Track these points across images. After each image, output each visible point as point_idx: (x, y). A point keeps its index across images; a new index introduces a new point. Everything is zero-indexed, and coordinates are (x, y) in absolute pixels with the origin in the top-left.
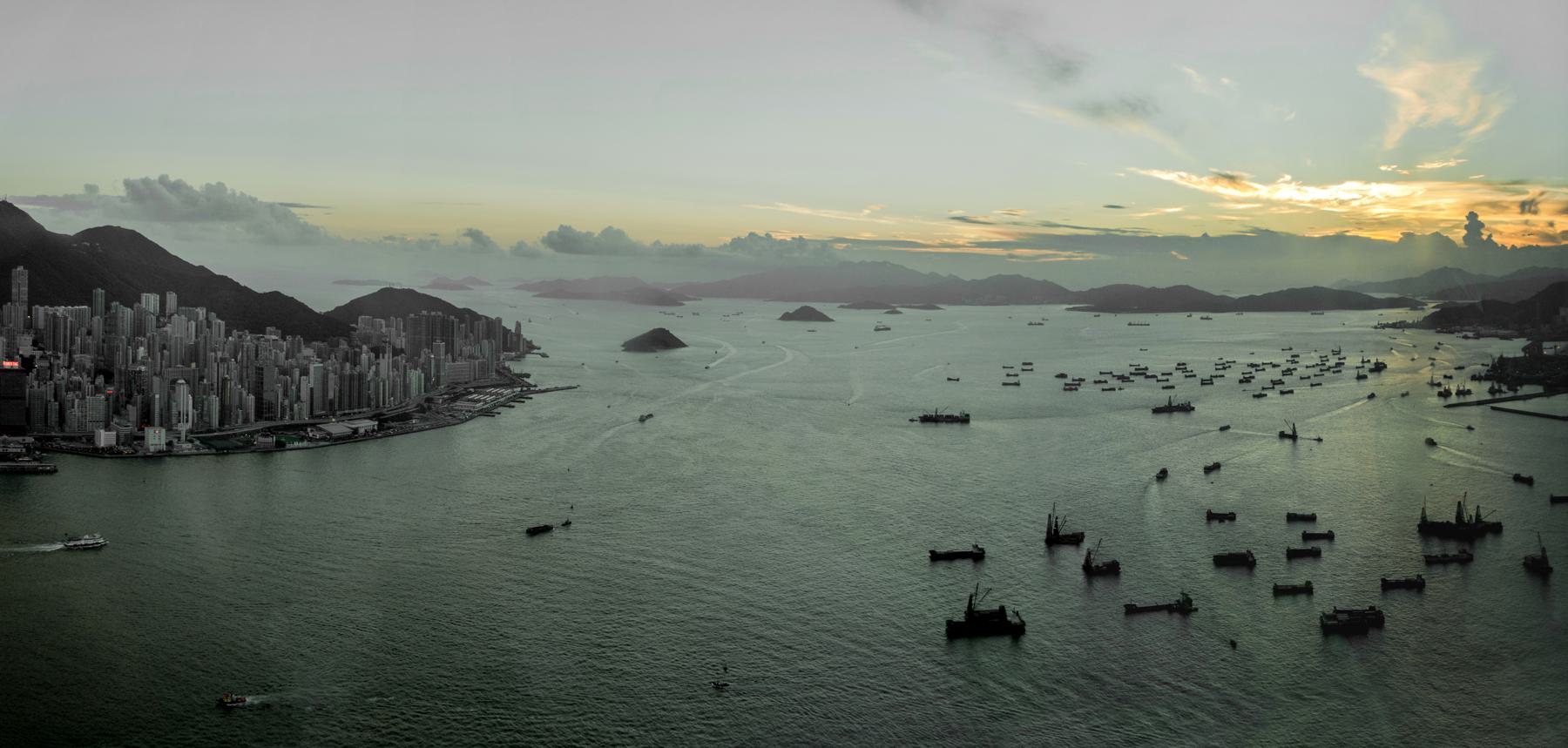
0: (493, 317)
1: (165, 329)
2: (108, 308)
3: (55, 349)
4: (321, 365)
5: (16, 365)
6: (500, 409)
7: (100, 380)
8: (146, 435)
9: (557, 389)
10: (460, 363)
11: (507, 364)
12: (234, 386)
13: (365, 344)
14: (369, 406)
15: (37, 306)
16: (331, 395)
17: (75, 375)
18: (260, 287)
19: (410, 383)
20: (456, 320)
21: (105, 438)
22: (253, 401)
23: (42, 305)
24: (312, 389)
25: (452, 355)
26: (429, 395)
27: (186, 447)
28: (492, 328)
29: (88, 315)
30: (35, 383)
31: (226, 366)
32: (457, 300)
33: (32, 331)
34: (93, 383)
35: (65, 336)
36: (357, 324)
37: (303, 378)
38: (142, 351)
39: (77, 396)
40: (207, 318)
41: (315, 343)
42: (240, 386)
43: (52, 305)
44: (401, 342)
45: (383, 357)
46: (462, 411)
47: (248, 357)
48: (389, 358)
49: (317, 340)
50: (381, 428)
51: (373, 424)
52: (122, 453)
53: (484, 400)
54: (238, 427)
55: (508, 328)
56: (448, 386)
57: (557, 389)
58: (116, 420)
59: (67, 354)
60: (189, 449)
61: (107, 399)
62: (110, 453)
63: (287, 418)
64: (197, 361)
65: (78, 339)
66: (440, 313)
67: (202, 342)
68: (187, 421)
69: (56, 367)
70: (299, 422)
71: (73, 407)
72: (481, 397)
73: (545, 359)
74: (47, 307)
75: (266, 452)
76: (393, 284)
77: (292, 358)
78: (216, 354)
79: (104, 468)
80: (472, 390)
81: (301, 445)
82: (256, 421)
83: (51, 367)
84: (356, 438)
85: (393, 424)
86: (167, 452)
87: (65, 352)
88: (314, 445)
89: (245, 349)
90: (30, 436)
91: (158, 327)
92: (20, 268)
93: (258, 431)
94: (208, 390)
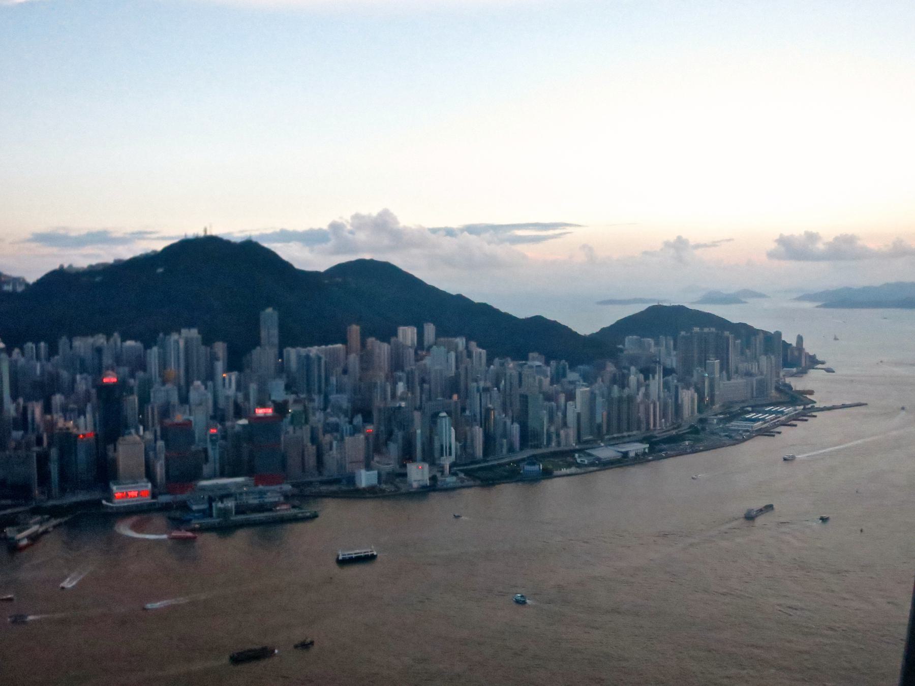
0: (772, 331)
1: (423, 362)
2: (363, 345)
3: (309, 391)
4: (588, 389)
5: (269, 411)
6: (781, 429)
7: (358, 419)
8: (408, 471)
9: (844, 406)
10: (735, 381)
11: (788, 380)
12: (497, 415)
13: (632, 364)
14: (639, 428)
15: (289, 349)
16: (599, 420)
17: (332, 416)
18: (522, 313)
19: (682, 404)
20: (731, 337)
21: (365, 478)
22: (518, 430)
23: (293, 346)
24: (579, 415)
25: (728, 372)
26: (702, 416)
27: (451, 480)
28: (772, 341)
29: (342, 355)
30: (290, 429)
31: (488, 395)
32: (732, 314)
33: (284, 376)
34: (351, 422)
35: (320, 376)
36: (624, 345)
37: (571, 403)
38: (401, 387)
39: (336, 438)
40: (467, 347)
41: (581, 367)
42: (504, 415)
43: (304, 345)
44: (672, 361)
45: (654, 378)
46: (739, 430)
47: (511, 383)
48: (659, 378)
49: (582, 364)
50: (652, 450)
51: (644, 447)
52: (383, 491)
53: (763, 419)
54: (504, 458)
55: (789, 342)
56: (723, 406)
57: (844, 406)
58: (376, 458)
59: (322, 396)
60: (453, 482)
61: (367, 438)
62: (372, 493)
63: (553, 444)
64: (458, 392)
65: (333, 380)
66: (713, 330)
67: (462, 372)
68: (450, 454)
69: (311, 411)
70: (567, 448)
71: (331, 449)
72: (760, 416)
73: (833, 373)
74: (299, 348)
75: (533, 479)
76: (662, 301)
77: (558, 382)
78: (478, 384)
79: (365, 509)
80: (750, 409)
81: (568, 471)
82: (521, 449)
83: (305, 411)
84: (627, 461)
85: (664, 446)
86: (430, 486)
87: (320, 392)
88: (583, 471)
89: (508, 377)
90: (287, 483)
91: (417, 360)
92: (269, 310)
93: (523, 460)
94: (471, 421)
